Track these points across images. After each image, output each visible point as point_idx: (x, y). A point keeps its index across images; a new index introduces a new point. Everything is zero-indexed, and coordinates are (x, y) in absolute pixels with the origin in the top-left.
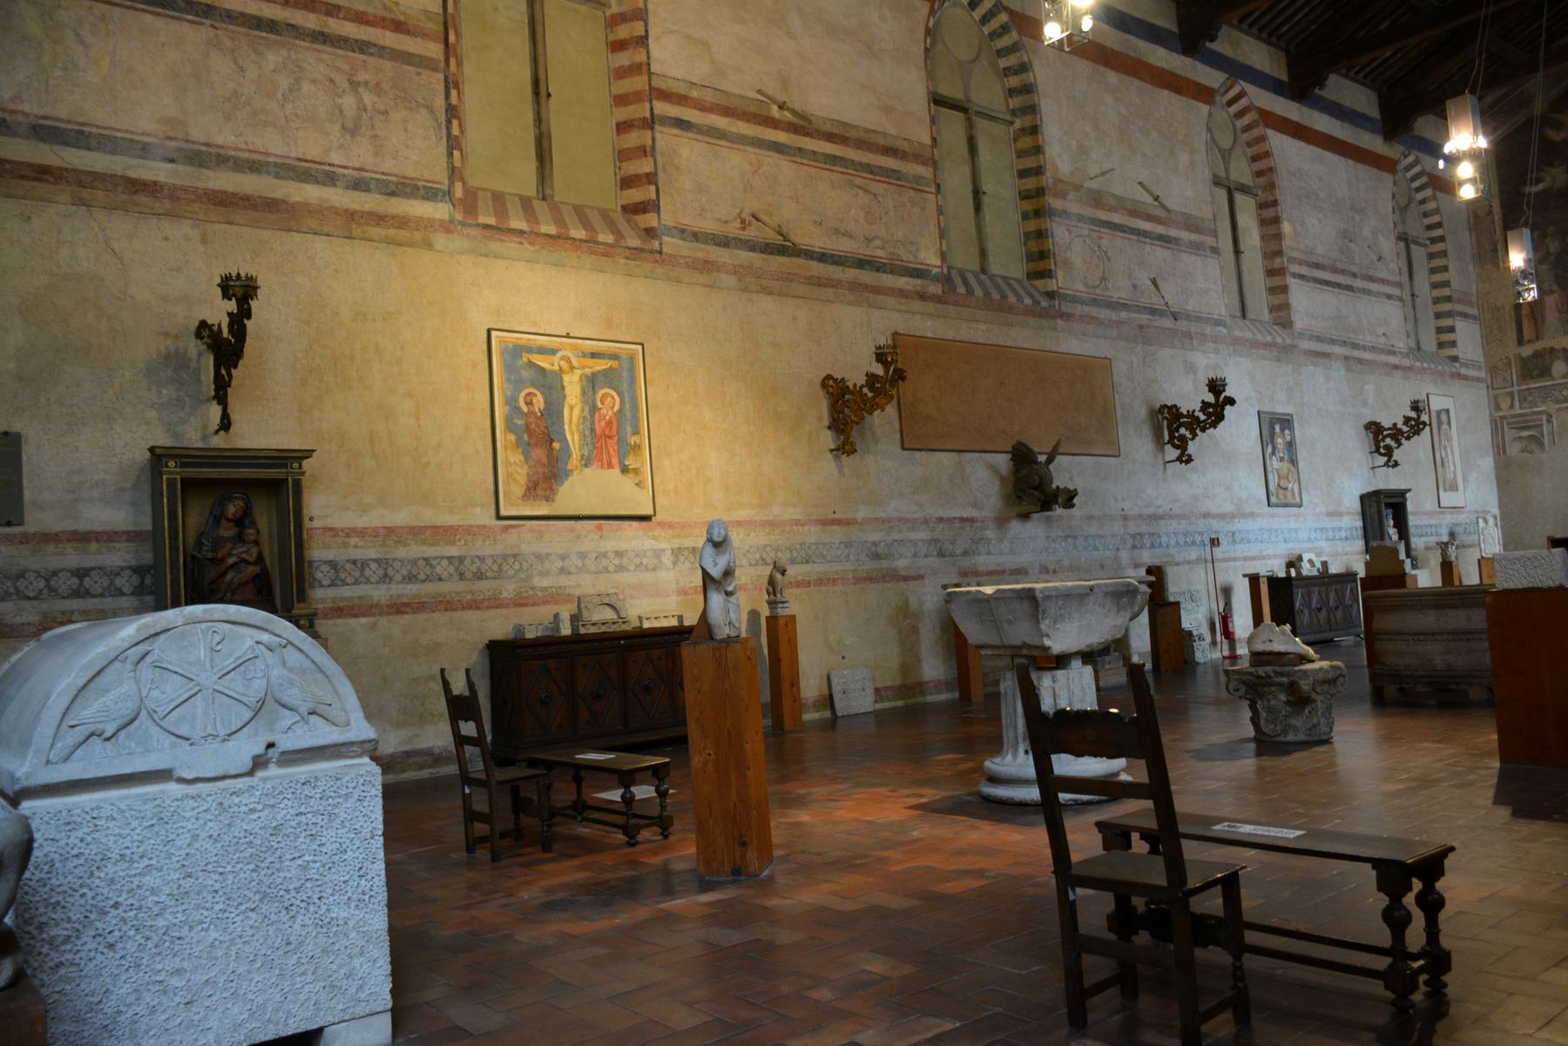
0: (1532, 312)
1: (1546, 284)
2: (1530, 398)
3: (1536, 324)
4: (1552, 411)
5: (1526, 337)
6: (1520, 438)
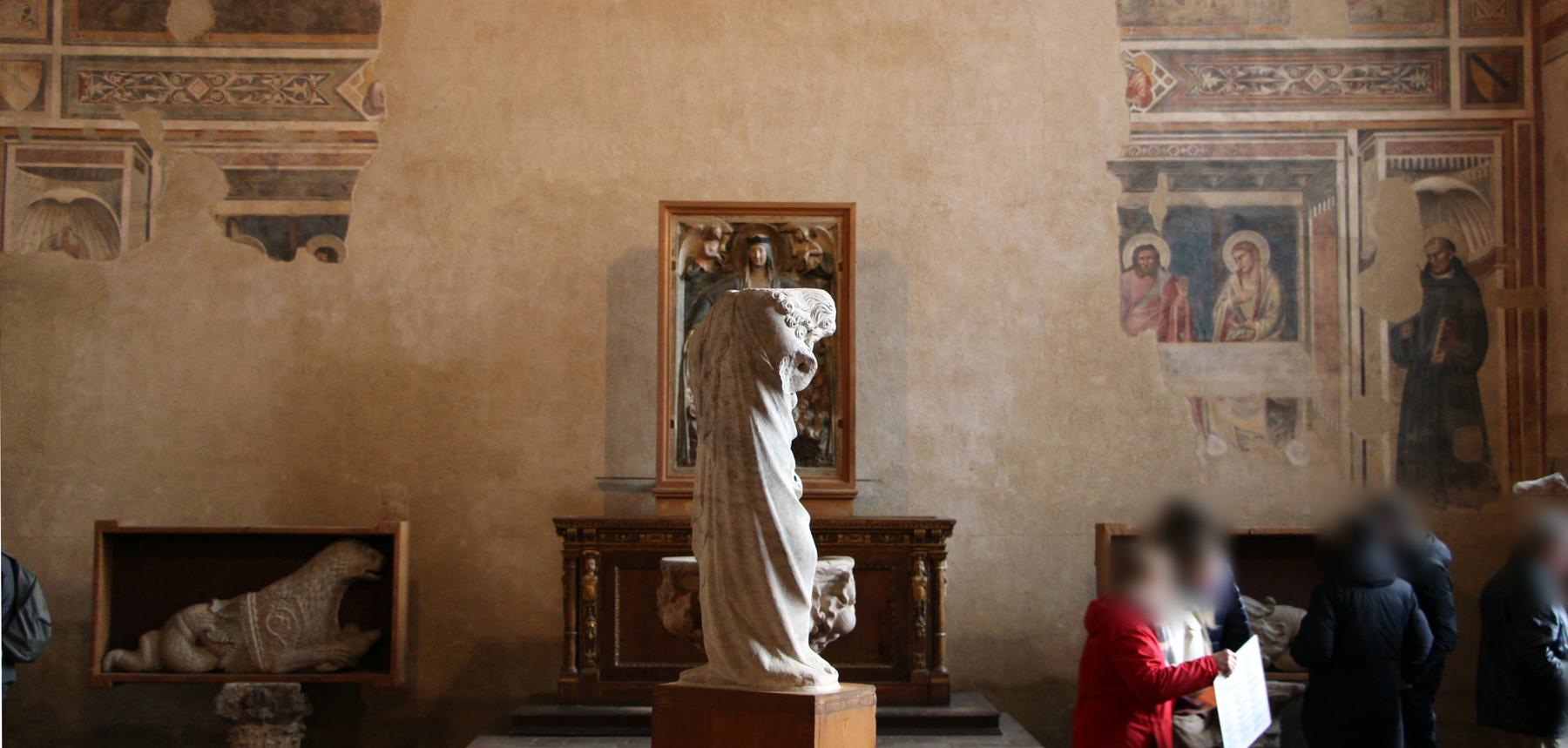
2: (94, 88)
4: (153, 137)
6: (51, 202)
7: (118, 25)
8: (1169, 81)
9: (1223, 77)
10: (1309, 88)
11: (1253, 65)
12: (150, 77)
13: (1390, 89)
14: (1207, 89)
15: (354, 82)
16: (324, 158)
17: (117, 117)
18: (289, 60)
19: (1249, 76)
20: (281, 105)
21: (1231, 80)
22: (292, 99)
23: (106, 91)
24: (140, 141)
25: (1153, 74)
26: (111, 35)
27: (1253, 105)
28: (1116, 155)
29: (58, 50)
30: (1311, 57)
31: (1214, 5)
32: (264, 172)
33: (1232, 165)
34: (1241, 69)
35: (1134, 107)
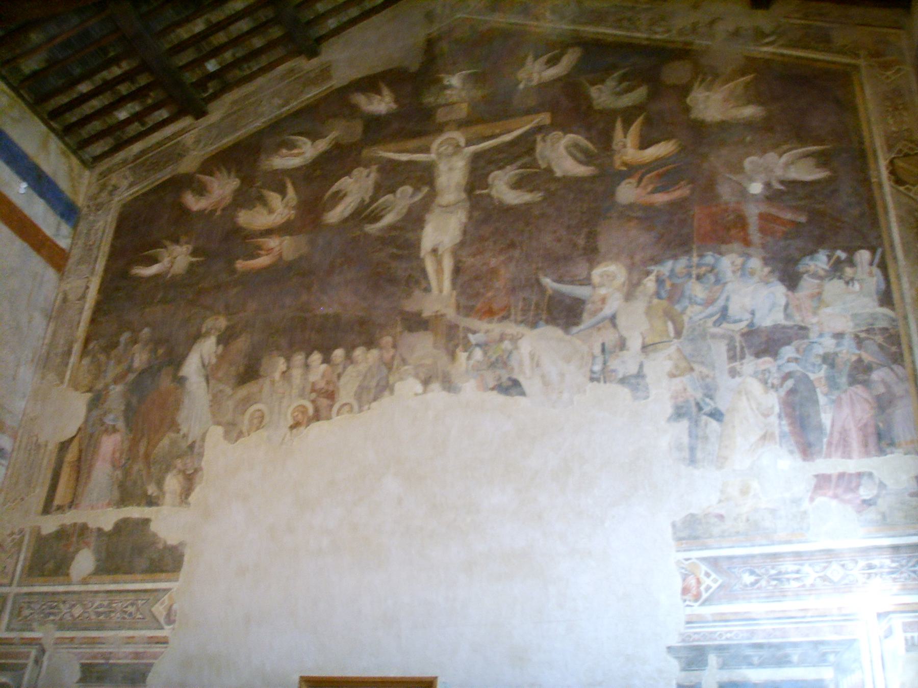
0: (79, 459)
1: (111, 416)
3: (77, 479)
4: (48, 643)
5: (57, 502)
7: (46, 573)
8: (715, 581)
9: (758, 575)
10: (831, 581)
11: (782, 565)
12: (55, 604)
13: (900, 578)
14: (746, 586)
15: (162, 604)
16: (137, 655)
17: (32, 630)
18: (128, 591)
19: (780, 573)
20: (119, 620)
21: (766, 577)
22: (126, 616)
23: (31, 614)
24: (41, 644)
25: (702, 577)
26: (42, 579)
27: (784, 596)
28: (675, 641)
29: (14, 589)
30: (829, 554)
31: (748, 520)
32: (102, 664)
33: (770, 646)
34: (773, 568)
35: (687, 603)
